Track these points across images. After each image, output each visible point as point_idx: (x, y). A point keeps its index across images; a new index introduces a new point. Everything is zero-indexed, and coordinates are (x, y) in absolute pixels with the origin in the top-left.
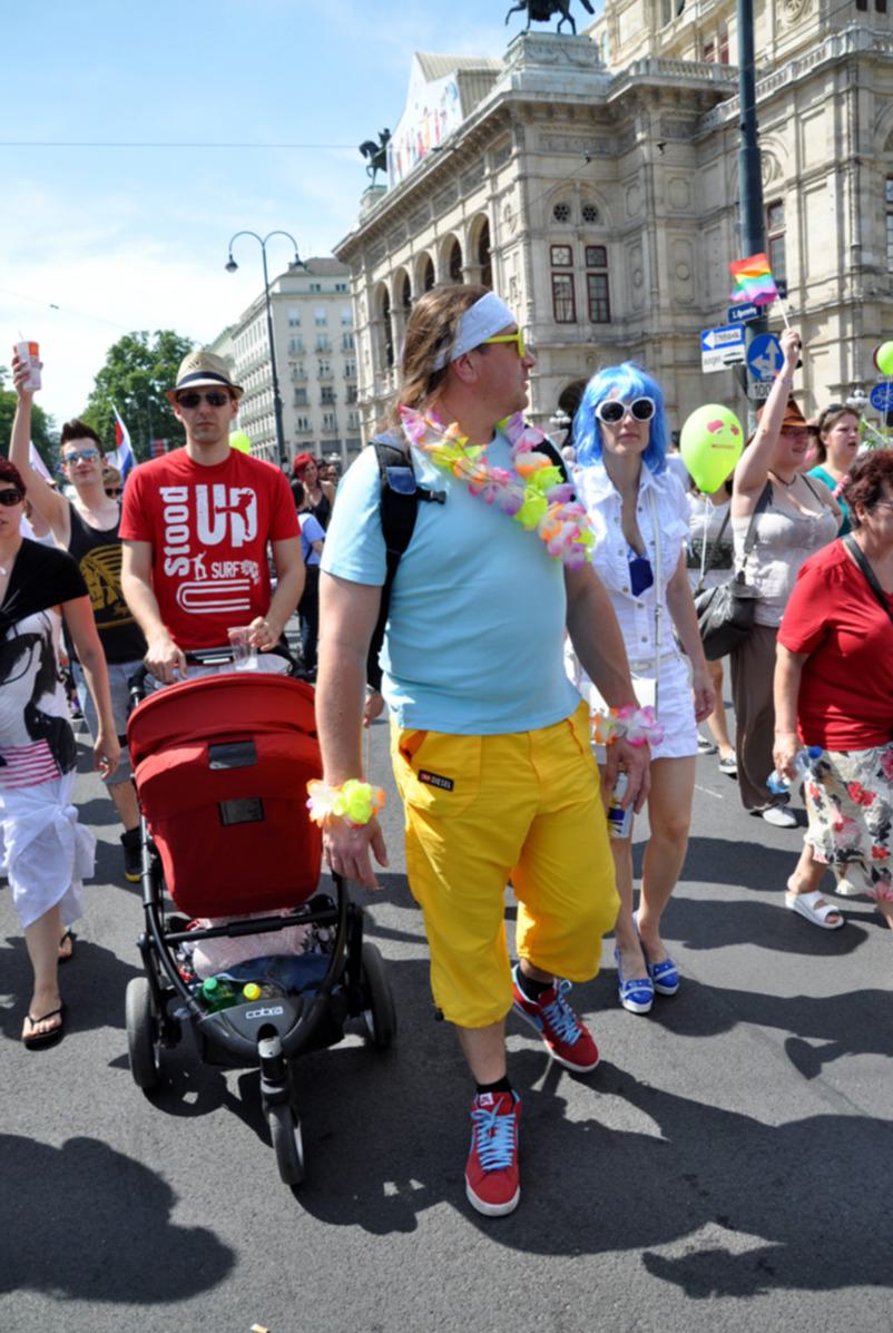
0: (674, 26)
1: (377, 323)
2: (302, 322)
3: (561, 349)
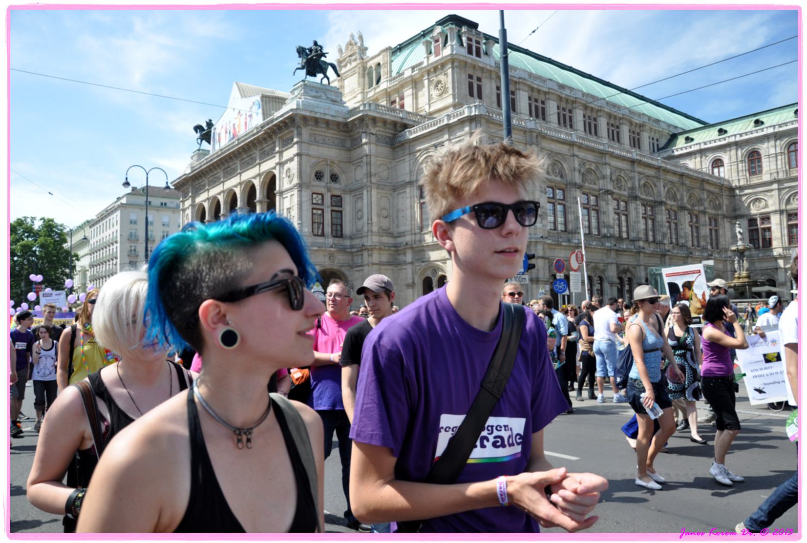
0: (375, 89)
3: (317, 250)
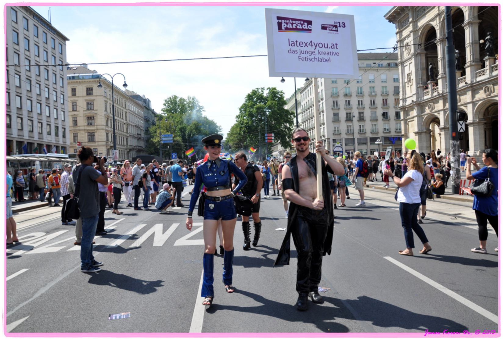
1: (420, 54)
2: (338, 81)
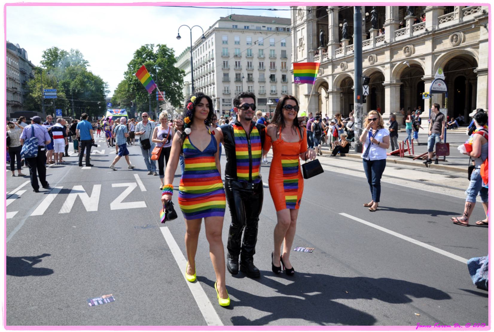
2: (229, 42)
